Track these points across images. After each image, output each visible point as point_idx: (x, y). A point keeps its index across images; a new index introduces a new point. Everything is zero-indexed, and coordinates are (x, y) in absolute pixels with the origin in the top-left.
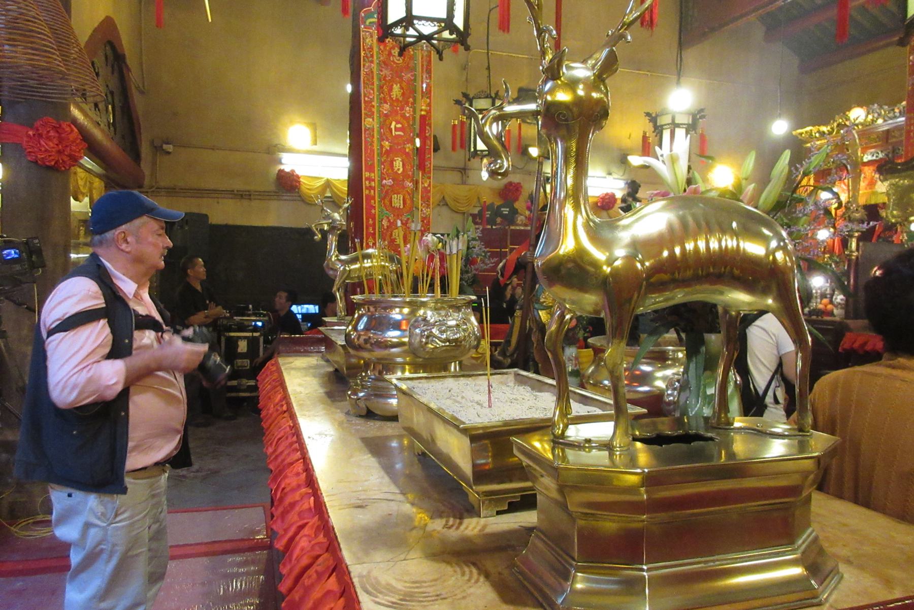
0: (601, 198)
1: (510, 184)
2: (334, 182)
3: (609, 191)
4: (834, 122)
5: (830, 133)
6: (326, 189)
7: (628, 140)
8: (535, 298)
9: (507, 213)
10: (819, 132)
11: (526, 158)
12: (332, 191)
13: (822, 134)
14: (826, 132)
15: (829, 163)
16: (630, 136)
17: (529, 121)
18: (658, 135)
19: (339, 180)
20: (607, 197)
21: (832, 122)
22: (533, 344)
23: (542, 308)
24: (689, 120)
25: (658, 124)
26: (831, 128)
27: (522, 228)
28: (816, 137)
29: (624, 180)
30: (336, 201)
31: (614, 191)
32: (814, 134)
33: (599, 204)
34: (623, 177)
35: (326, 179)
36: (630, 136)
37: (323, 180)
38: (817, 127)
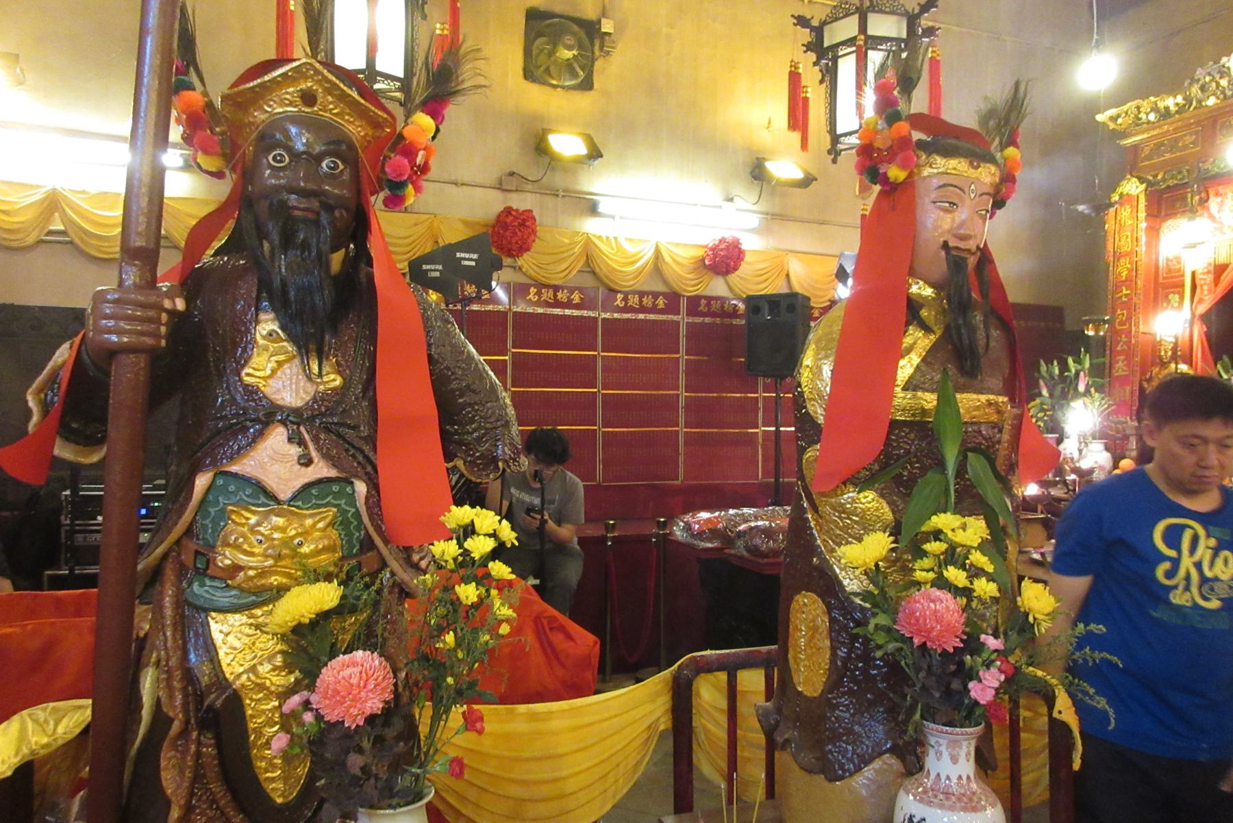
0: (712, 249)
1: (508, 211)
2: (70, 196)
3: (729, 235)
4: (1191, 84)
5: (1181, 109)
6: (52, 214)
7: (766, 132)
8: (192, 545)
9: (473, 263)
10: (1155, 109)
11: (546, 160)
12: (66, 219)
13: (1166, 114)
14: (1173, 109)
15: (1180, 172)
16: (769, 123)
17: (554, 82)
18: (827, 78)
19: (83, 192)
20: (723, 246)
21: (1186, 84)
22: (168, 804)
23: (224, 598)
24: (900, 30)
25: (826, 45)
26: (1184, 99)
27: (540, 310)
28: (1149, 122)
29: (762, 213)
30: (77, 241)
31: (738, 235)
32: (1143, 116)
33: (707, 262)
34: (755, 208)
35: (50, 187)
36: (769, 123)
37: (43, 190)
38: (1152, 99)
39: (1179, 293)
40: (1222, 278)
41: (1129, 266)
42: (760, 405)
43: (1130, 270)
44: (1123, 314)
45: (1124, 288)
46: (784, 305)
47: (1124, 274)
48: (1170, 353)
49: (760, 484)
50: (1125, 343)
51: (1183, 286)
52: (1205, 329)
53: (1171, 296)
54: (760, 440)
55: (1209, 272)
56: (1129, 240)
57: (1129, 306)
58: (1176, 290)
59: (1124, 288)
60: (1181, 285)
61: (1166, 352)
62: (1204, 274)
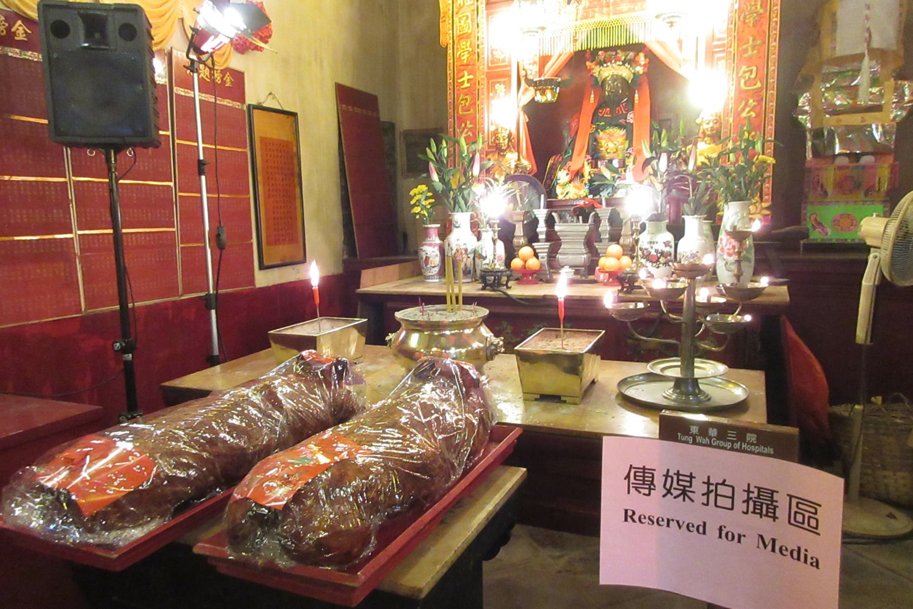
39: (504, 83)
40: (546, 68)
41: (470, 50)
42: (71, 195)
43: (472, 53)
44: (466, 99)
45: (466, 73)
46: (112, 29)
47: (465, 57)
48: (506, 141)
49: (82, 319)
50: (470, 129)
51: (509, 76)
52: (527, 120)
53: (497, 86)
54: (77, 251)
55: (535, 63)
56: (469, 21)
57: (473, 92)
58: (503, 80)
59: (466, 73)
60: (507, 75)
61: (504, 139)
62: (530, 64)
